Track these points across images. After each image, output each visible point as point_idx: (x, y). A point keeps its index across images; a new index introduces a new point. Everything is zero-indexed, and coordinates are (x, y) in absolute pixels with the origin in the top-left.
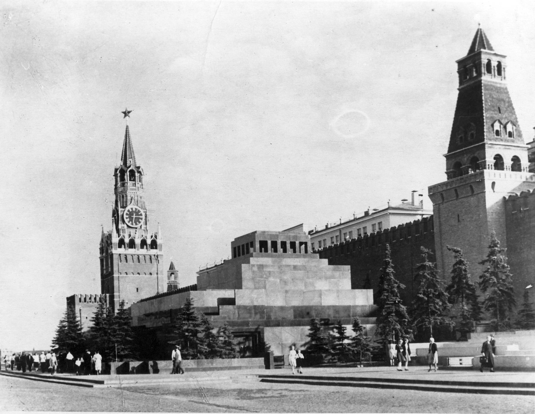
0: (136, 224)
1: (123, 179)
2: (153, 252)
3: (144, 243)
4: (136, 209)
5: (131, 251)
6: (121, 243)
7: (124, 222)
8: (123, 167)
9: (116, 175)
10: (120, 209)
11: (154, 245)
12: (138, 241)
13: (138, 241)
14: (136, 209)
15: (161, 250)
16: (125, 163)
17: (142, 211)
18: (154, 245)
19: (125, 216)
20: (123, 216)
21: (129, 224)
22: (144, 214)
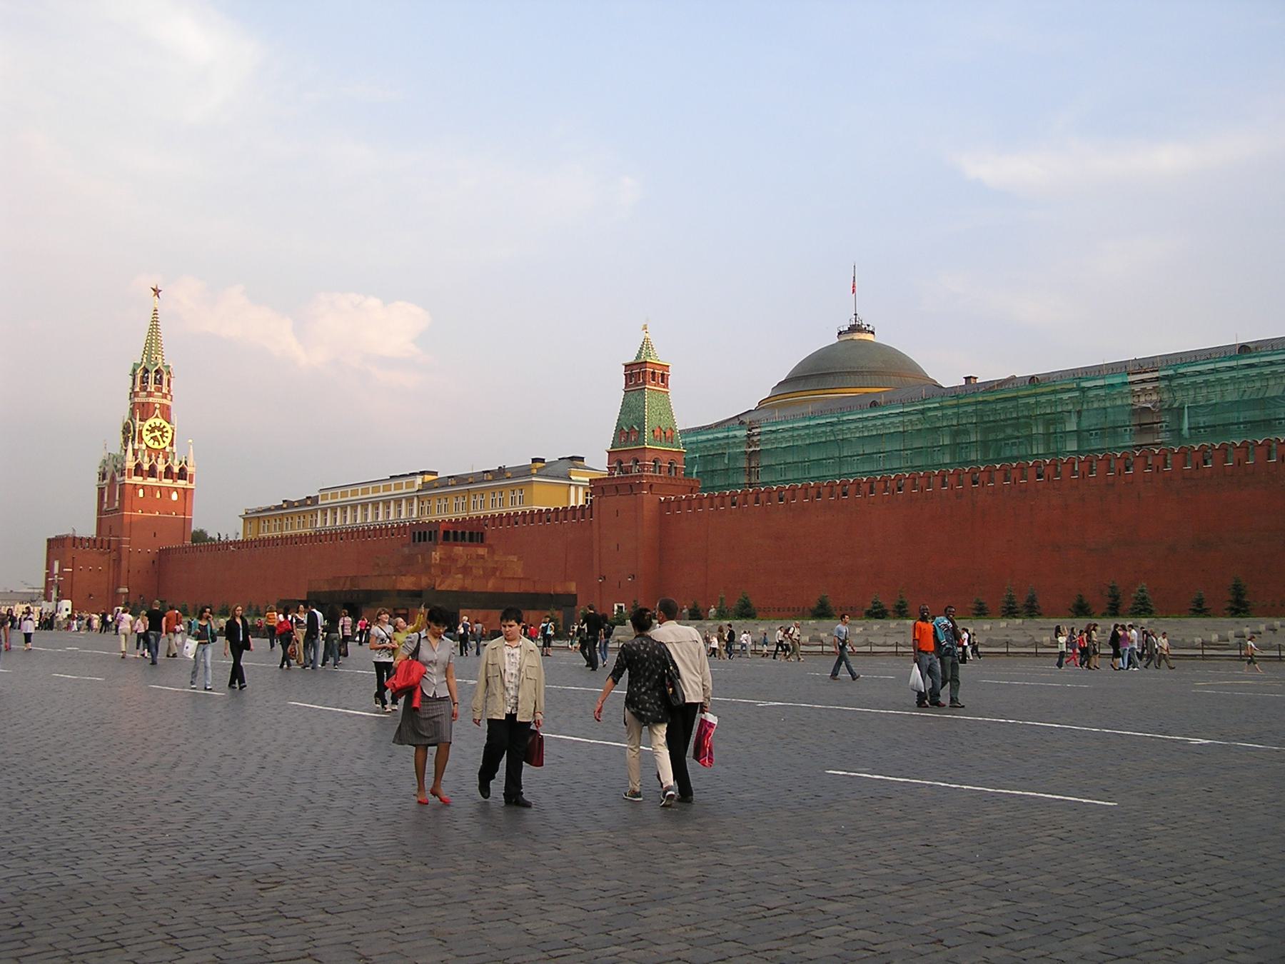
1: (144, 380)
2: (181, 483)
3: (168, 473)
5: (151, 481)
6: (138, 470)
7: (141, 439)
9: (134, 374)
10: (138, 423)
11: (182, 474)
12: (161, 467)
13: (161, 467)
17: (168, 427)
18: (182, 474)
19: (144, 433)
20: (141, 432)
21: (150, 444)
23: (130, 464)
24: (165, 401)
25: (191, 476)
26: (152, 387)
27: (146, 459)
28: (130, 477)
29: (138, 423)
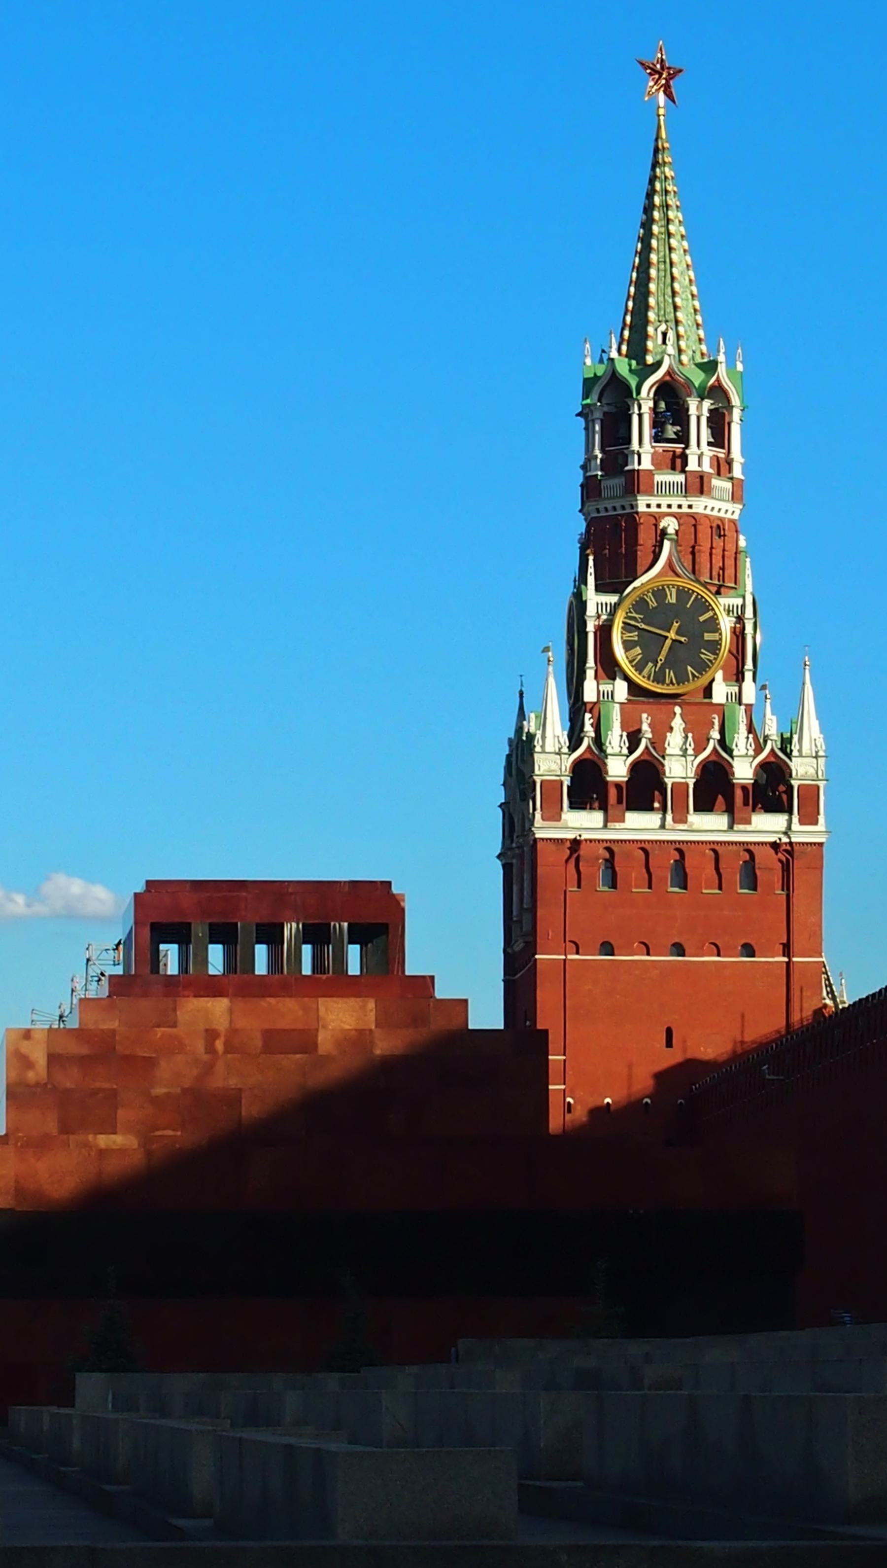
0: (682, 679)
1: (615, 430)
2: (766, 826)
3: (712, 786)
4: (683, 594)
5: (640, 825)
6: (585, 785)
7: (609, 668)
8: (623, 367)
10: (594, 600)
11: (773, 788)
12: (680, 769)
13: (680, 769)
14: (683, 594)
15: (809, 818)
16: (637, 347)
18: (773, 788)
22: (726, 623)
23: (552, 763)
24: (701, 505)
25: (811, 794)
26: (645, 452)
27: (615, 739)
28: (553, 814)
29: (596, 601)
